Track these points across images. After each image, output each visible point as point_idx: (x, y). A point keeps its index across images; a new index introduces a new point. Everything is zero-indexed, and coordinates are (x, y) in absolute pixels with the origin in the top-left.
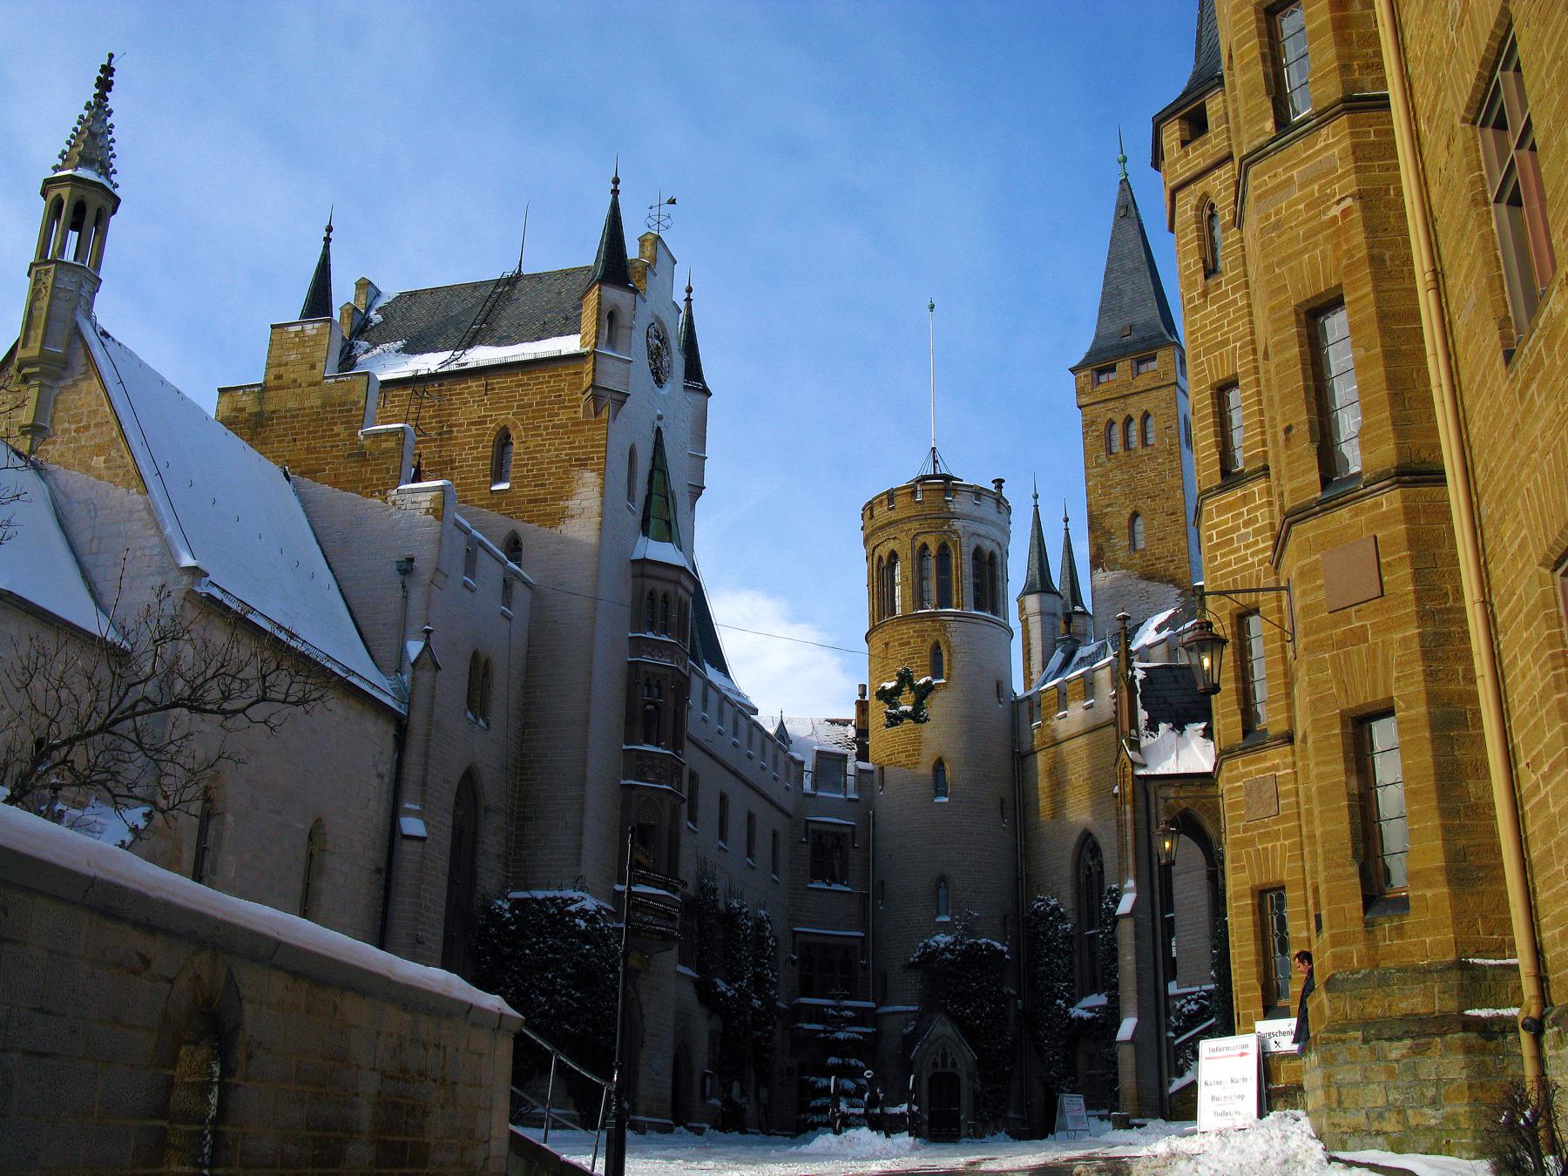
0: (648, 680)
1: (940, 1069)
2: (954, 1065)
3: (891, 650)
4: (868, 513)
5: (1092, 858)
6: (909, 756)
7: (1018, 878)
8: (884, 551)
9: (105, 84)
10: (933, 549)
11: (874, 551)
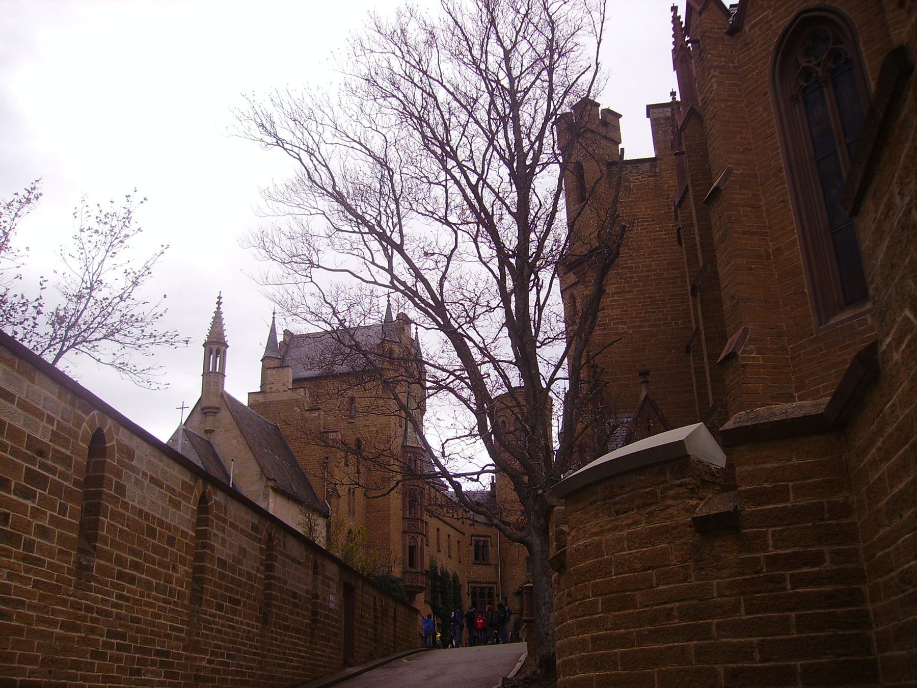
9: (219, 303)
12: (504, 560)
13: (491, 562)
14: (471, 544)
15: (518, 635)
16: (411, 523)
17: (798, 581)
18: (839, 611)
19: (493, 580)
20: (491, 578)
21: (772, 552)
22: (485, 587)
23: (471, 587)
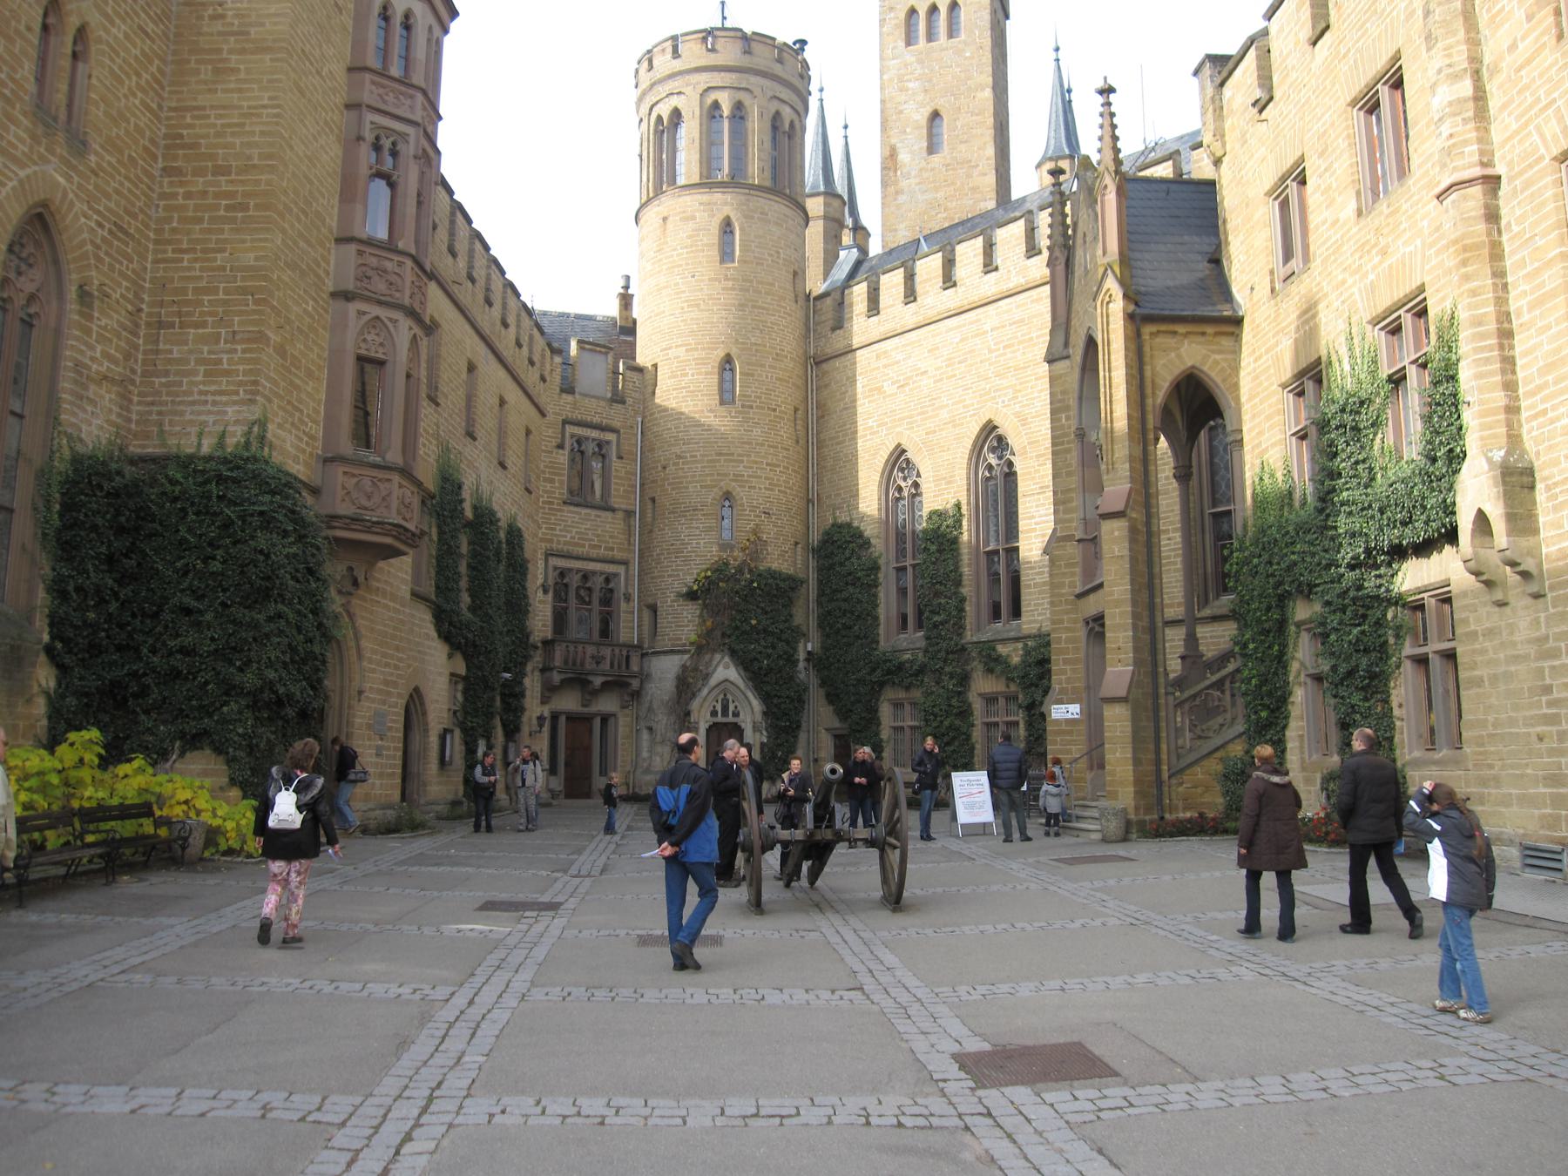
0: (377, 138)
1: (720, 719)
2: (736, 714)
3: (670, 225)
4: (645, 64)
5: (905, 479)
6: (691, 350)
7: (808, 501)
8: (664, 110)
10: (726, 110)
11: (651, 109)
12: (653, 500)
13: (615, 501)
14: (561, 446)
15: (688, 714)
16: (373, 261)
19: (618, 555)
20: (612, 549)
22: (594, 573)
23: (555, 568)
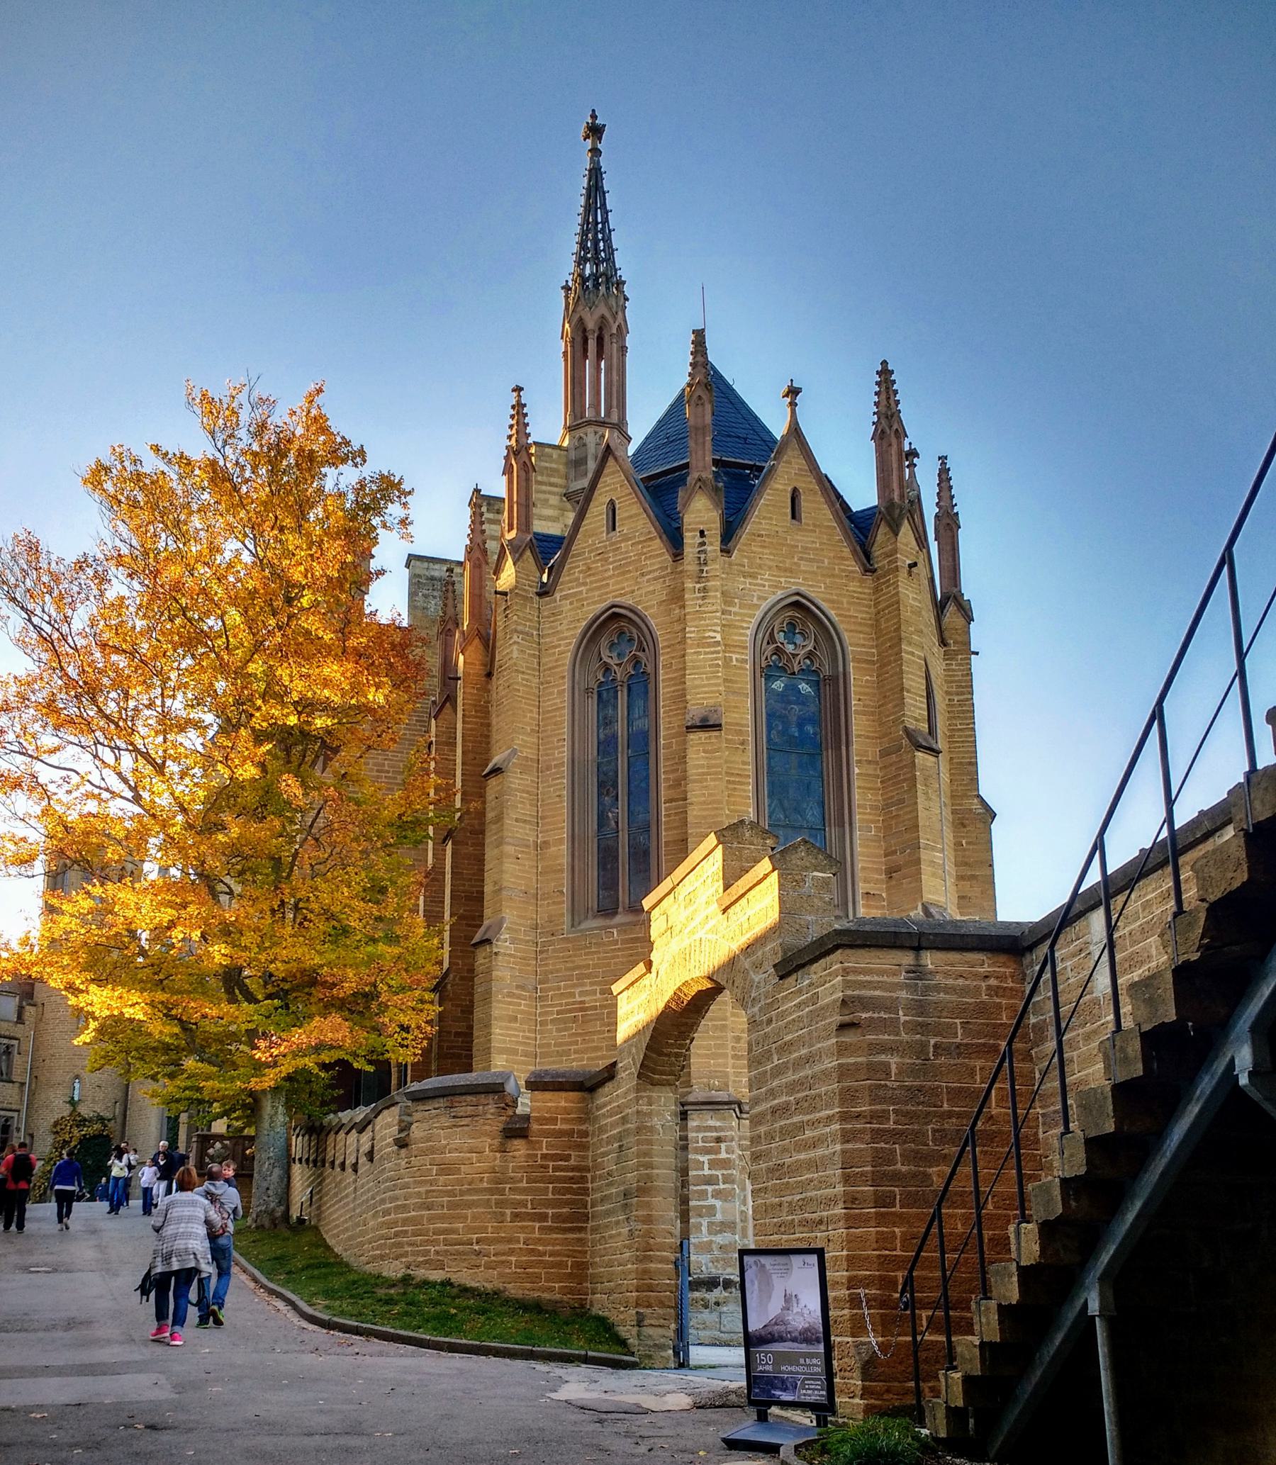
17: (556, 1169)
18: (574, 1186)
21: (545, 1151)
